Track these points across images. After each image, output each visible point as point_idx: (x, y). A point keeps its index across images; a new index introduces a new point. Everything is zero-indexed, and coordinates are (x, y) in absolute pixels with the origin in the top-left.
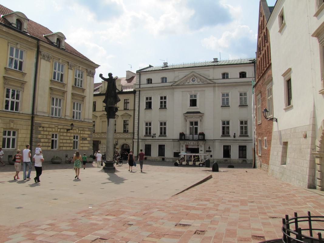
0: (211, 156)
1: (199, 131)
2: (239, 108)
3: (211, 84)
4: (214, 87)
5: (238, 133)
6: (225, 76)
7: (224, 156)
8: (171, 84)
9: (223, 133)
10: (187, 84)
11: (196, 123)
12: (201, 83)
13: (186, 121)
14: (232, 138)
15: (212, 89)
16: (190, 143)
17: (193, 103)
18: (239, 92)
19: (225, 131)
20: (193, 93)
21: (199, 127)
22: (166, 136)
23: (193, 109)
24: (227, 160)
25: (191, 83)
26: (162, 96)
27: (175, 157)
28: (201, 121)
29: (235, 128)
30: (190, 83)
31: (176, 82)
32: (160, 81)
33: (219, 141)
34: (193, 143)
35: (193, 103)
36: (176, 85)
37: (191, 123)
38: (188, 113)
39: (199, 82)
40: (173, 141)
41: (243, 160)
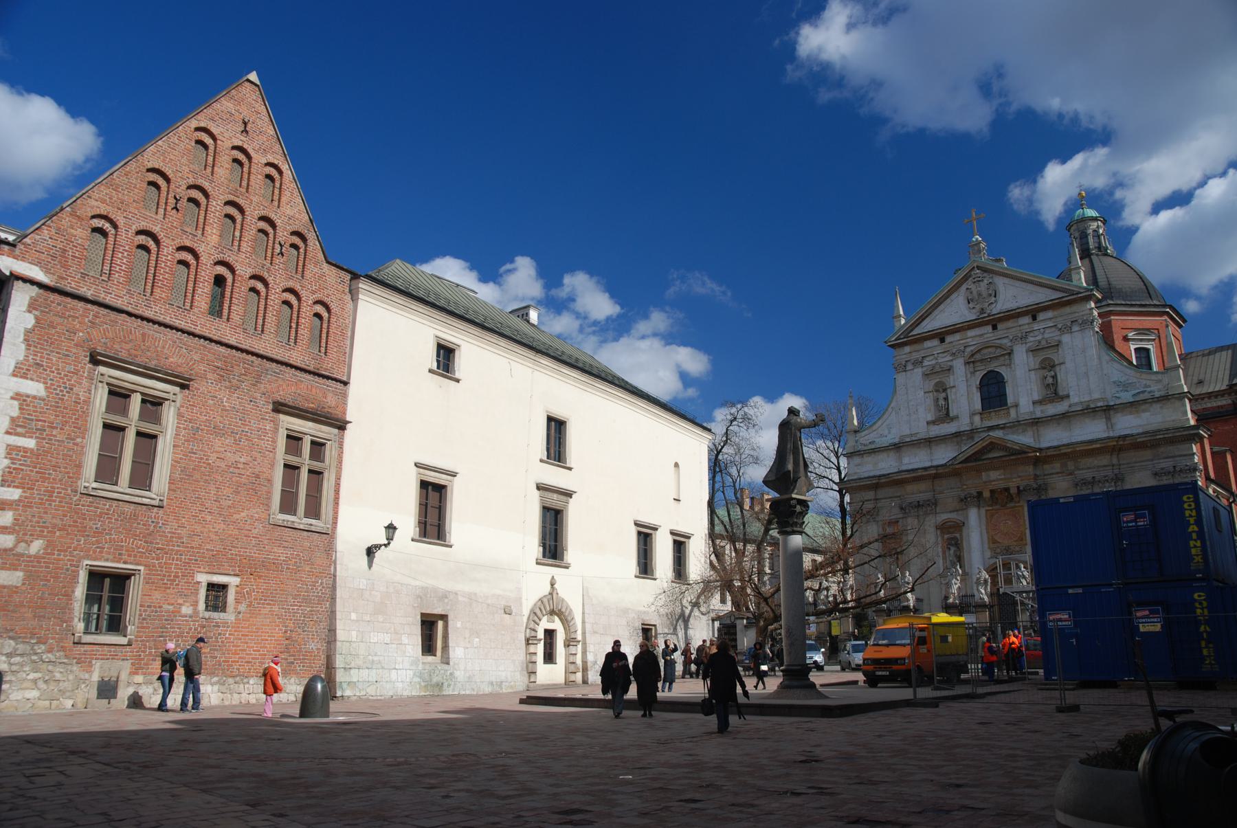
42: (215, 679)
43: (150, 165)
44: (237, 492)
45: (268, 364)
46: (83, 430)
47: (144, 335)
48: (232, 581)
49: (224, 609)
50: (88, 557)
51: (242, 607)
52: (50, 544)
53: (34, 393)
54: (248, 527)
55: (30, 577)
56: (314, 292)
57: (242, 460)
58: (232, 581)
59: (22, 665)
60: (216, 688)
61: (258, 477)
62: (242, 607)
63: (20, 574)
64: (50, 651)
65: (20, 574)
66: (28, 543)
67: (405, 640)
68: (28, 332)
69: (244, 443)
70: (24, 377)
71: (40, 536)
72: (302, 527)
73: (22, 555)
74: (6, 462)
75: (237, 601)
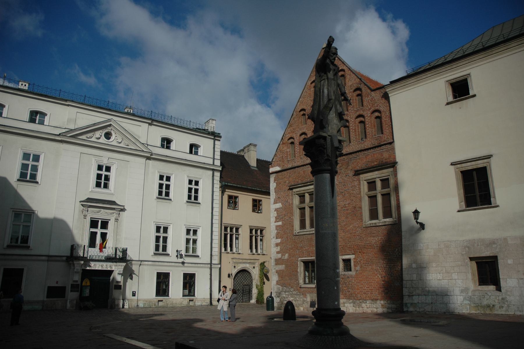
0: (134, 294)
1: (110, 243)
2: (185, 205)
3: (143, 151)
4: (148, 158)
5: (183, 253)
6: (166, 143)
7: (158, 294)
8: (58, 132)
9: (157, 248)
10: (93, 139)
11: (105, 224)
12: (121, 145)
13: (85, 216)
14: (173, 258)
15: (144, 160)
16: (95, 265)
17: (102, 181)
18: (188, 176)
19: (161, 245)
20: (105, 162)
21: (110, 231)
22: (28, 247)
23: (101, 194)
24: (162, 301)
25: (103, 140)
26: (28, 152)
27: (48, 299)
28: (117, 220)
29: (176, 241)
30: (100, 141)
31: (72, 130)
32: (27, 117)
33: (150, 263)
34: (102, 266)
35: (102, 181)
36: (70, 136)
37: (94, 224)
38: (89, 200)
39: (120, 143)
40: (48, 261)
41: (190, 300)
42: (351, 301)
43: (299, 110)
44: (347, 218)
45: (350, 156)
46: (292, 214)
47: (304, 172)
48: (352, 257)
49: (351, 270)
50: (300, 257)
51: (358, 268)
52: (289, 255)
53: (278, 207)
54: (354, 232)
55: (286, 267)
56: (370, 109)
57: (347, 203)
58: (352, 257)
59: (288, 295)
60: (352, 305)
61: (355, 208)
62: (358, 268)
63: (284, 266)
64: (294, 290)
65: (284, 266)
66: (284, 255)
67: (455, 276)
68: (275, 189)
69: (347, 195)
70: (276, 203)
71: (287, 253)
72: (380, 224)
73: (283, 260)
74: (276, 231)
75: (355, 266)
